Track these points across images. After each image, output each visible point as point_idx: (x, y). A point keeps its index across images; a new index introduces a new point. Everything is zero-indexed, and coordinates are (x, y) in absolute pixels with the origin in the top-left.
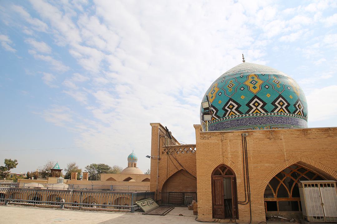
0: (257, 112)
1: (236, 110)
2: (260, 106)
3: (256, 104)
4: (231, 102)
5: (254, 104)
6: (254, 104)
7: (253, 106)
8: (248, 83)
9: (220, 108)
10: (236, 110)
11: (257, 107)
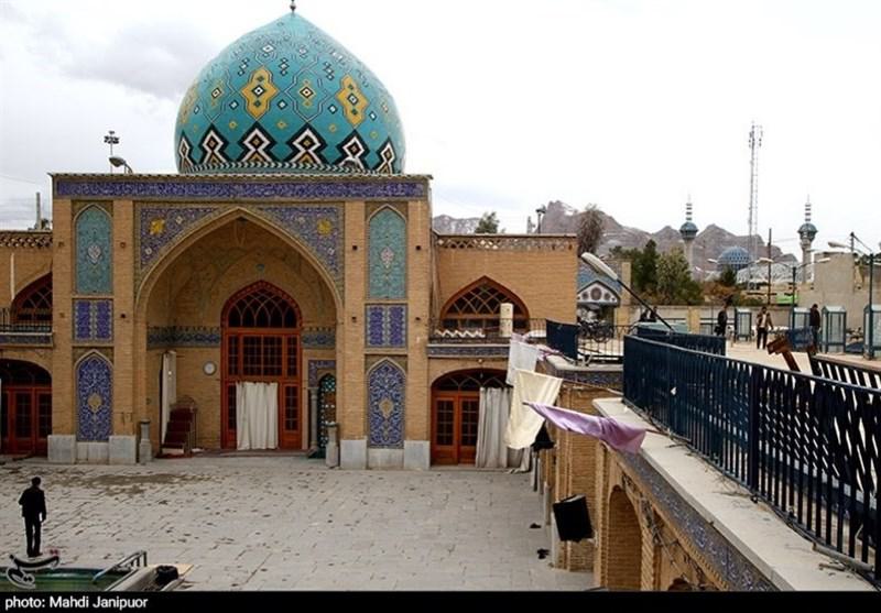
2: (264, 146)
3: (256, 142)
8: (246, 92)
11: (256, 147)
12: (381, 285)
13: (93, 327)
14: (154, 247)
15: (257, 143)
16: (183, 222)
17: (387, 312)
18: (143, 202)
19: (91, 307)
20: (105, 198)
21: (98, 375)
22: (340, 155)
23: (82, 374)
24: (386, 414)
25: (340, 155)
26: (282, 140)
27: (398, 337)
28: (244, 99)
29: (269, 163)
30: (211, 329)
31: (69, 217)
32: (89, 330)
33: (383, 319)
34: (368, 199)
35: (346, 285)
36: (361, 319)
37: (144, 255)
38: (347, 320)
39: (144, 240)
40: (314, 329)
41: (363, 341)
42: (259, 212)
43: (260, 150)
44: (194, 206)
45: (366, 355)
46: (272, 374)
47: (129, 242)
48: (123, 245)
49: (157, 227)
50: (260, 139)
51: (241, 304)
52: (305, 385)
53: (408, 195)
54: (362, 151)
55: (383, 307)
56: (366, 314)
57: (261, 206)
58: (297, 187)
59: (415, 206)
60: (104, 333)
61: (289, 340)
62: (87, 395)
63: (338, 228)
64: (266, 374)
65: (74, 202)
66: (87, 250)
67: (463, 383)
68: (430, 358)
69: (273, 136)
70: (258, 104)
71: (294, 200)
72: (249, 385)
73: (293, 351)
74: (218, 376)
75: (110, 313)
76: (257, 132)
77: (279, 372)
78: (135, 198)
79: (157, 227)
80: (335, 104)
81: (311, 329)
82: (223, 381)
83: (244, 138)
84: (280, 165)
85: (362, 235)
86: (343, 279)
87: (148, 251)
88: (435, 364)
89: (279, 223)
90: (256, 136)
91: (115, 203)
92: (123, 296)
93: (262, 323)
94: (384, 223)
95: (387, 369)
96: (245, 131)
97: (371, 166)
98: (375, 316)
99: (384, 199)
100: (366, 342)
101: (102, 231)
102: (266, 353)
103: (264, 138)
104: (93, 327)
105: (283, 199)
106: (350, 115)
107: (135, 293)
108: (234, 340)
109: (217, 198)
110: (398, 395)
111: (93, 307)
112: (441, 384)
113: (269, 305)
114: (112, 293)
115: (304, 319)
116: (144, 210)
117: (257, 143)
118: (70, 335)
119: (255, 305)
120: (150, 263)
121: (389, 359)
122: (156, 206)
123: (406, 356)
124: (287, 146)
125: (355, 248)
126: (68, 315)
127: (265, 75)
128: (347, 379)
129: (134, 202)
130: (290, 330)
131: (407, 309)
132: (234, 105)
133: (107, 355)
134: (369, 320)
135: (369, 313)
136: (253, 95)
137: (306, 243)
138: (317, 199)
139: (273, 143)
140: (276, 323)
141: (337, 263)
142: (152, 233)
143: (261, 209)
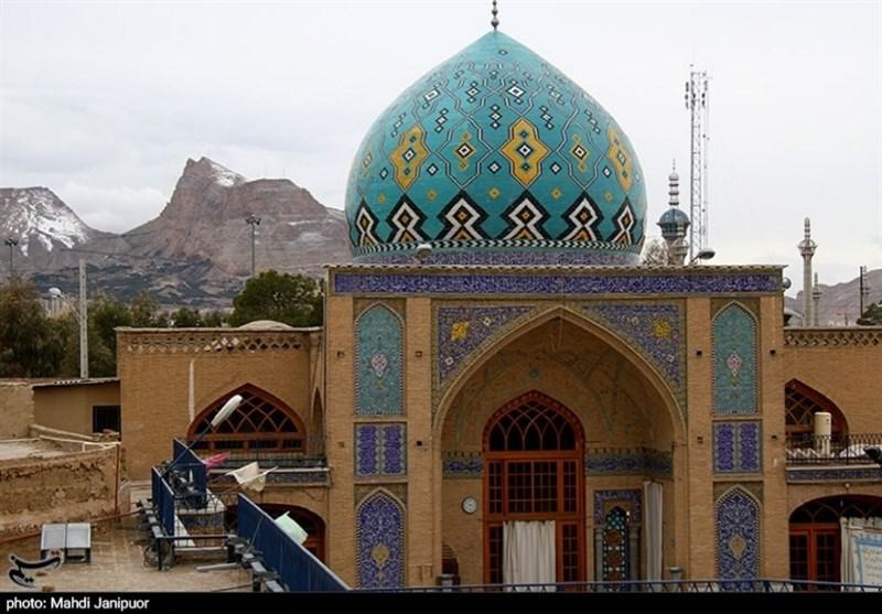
0: (525, 237)
1: (475, 226)
4: (462, 202)
5: (519, 216)
6: (519, 216)
7: (518, 221)
8: (509, 150)
9: (432, 214)
10: (475, 226)
11: (526, 222)
12: (727, 397)
13: (380, 459)
14: (454, 354)
15: (526, 216)
16: (492, 324)
17: (737, 431)
18: (442, 300)
19: (377, 433)
20: (397, 294)
21: (384, 519)
22: (567, 227)
23: (363, 521)
24: (737, 554)
25: (567, 227)
26: (556, 213)
27: (751, 460)
28: (505, 165)
29: (539, 241)
30: (471, 455)
31: (351, 318)
32: (375, 462)
33: (734, 439)
34: (715, 294)
35: (690, 399)
36: (708, 439)
37: (443, 365)
38: (692, 441)
39: (444, 346)
40: (601, 451)
41: (710, 465)
42: (584, 311)
43: (530, 225)
44: (506, 304)
45: (715, 483)
46: (546, 510)
47: (426, 349)
48: (419, 354)
49: (459, 331)
50: (530, 212)
51: (505, 422)
52: (590, 522)
53: (760, 290)
54: (595, 218)
55: (733, 424)
56: (713, 433)
57: (586, 304)
58: (631, 282)
59: (768, 304)
60: (393, 468)
61: (566, 465)
62: (371, 547)
63: (679, 333)
64: (537, 510)
65: (356, 300)
66: (370, 360)
67: (816, 513)
68: (789, 484)
69: (548, 209)
70: (526, 167)
71: (627, 296)
72: (519, 525)
73: (570, 480)
74: (480, 515)
75: (401, 441)
76: (527, 202)
77: (554, 507)
78: (434, 295)
79: (459, 331)
80: (559, 161)
81: (596, 450)
82: (486, 522)
83: (511, 209)
84: (552, 243)
85: (707, 338)
86: (686, 391)
87: (449, 361)
88: (794, 490)
89: (608, 324)
90: (526, 208)
91: (409, 301)
92: (420, 420)
93: (533, 444)
94: (730, 323)
95: (737, 499)
96: (511, 201)
97: (605, 237)
98: (724, 433)
99: (734, 295)
100: (714, 467)
101: (389, 336)
102: (537, 482)
103: (521, 207)
104: (380, 459)
105: (615, 296)
106: (622, 177)
107: (433, 414)
108: (496, 468)
109: (535, 295)
110: (751, 531)
111: (380, 433)
112: (799, 516)
113: (541, 421)
114: (403, 414)
115: (588, 439)
116: (442, 310)
117: (526, 216)
118: (352, 470)
119: (524, 422)
120: (451, 375)
121: (385, 490)
122: (458, 304)
123: (762, 482)
124: (562, 221)
125: (699, 353)
126: (349, 443)
127: (529, 129)
128: (692, 513)
129: (433, 300)
130: (567, 453)
131: (761, 426)
132: (495, 167)
133: (397, 493)
134: (717, 439)
135: (717, 432)
136: (517, 155)
137: (640, 348)
138: (654, 295)
139: (546, 216)
140: (550, 445)
141: (678, 372)
142: (453, 338)
143: (586, 308)
